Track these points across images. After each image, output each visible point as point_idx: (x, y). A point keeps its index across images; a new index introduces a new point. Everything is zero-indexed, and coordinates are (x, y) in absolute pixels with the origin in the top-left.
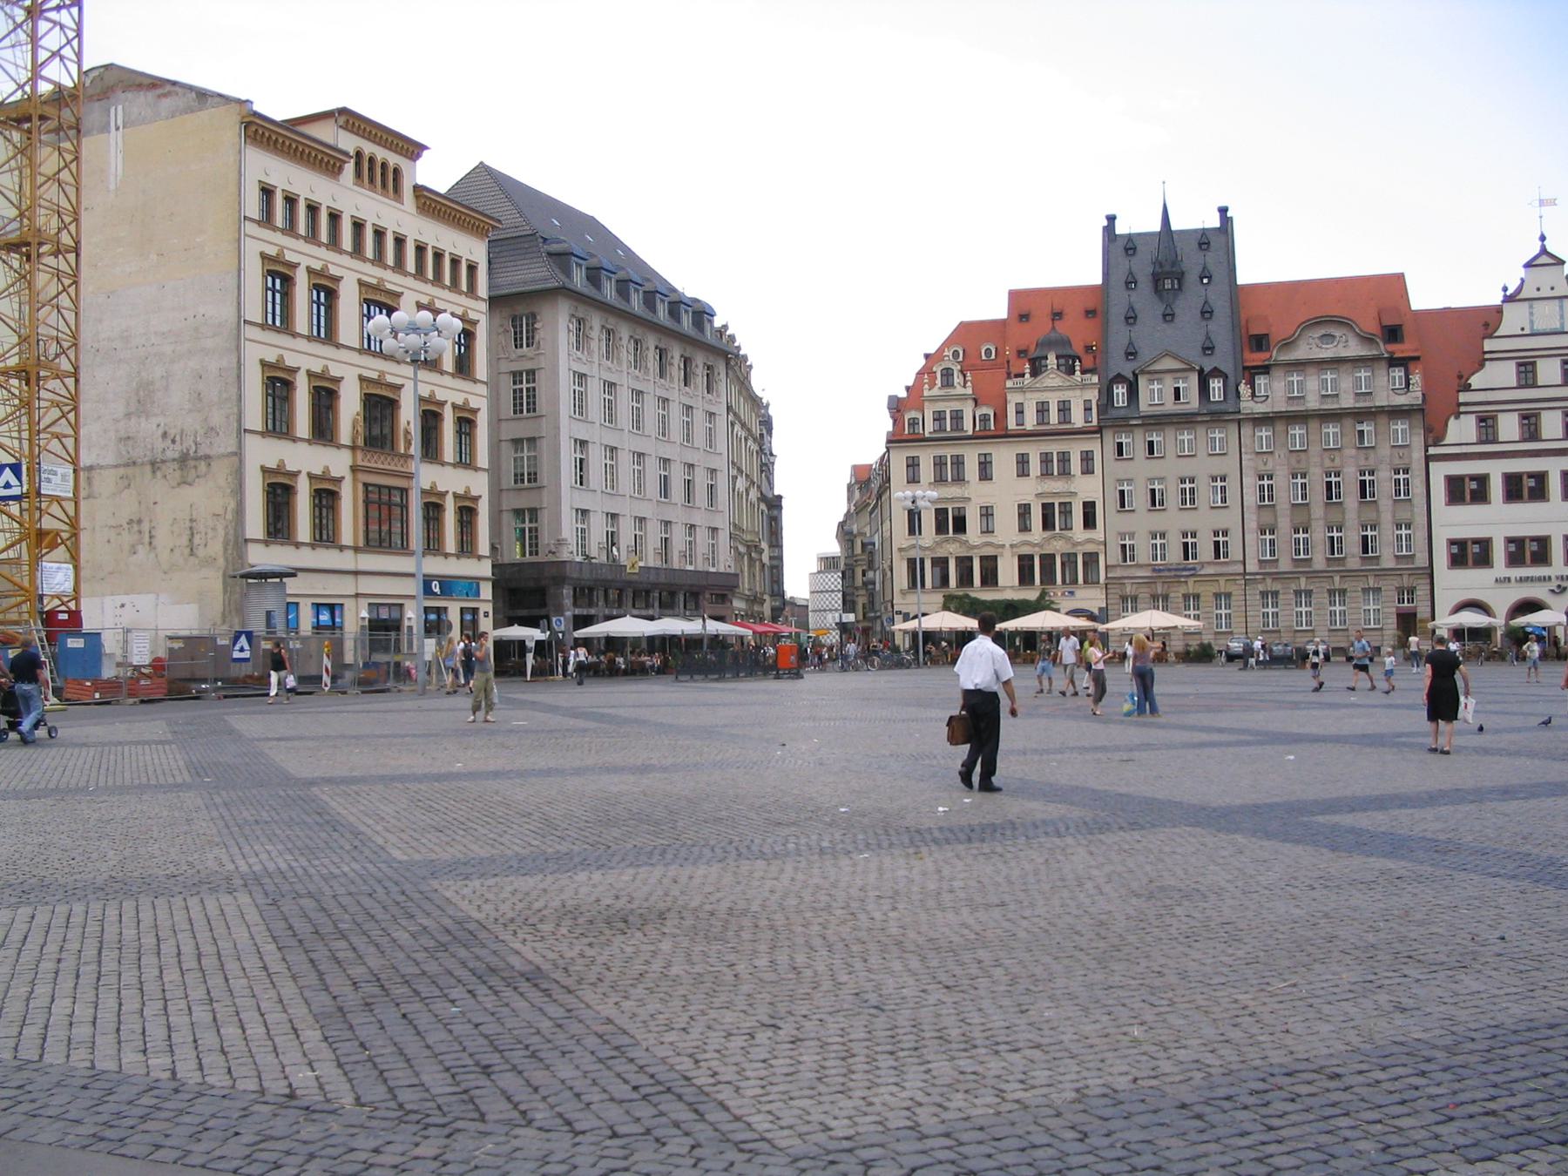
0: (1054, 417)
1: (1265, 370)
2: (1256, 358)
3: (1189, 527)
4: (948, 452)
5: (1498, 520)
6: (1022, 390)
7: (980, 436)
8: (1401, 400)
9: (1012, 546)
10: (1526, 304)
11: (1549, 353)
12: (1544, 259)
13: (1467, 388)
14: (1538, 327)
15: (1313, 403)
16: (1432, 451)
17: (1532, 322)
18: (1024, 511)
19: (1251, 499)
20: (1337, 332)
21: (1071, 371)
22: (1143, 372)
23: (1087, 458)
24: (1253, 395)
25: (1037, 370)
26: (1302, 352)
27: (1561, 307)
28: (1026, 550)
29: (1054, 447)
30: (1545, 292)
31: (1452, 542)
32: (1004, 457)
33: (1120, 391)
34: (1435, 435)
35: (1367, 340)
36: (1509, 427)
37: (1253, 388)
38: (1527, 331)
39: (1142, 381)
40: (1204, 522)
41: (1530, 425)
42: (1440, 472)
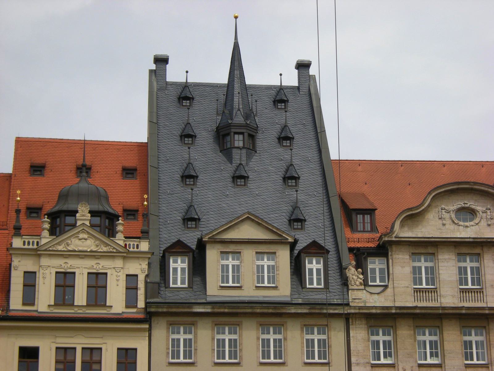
1: (382, 250)
2: (363, 239)
6: (36, 253)
15: (449, 298)
21: (111, 233)
22: (215, 241)
24: (365, 283)
26: (432, 227)
29: (79, 342)
37: (364, 273)
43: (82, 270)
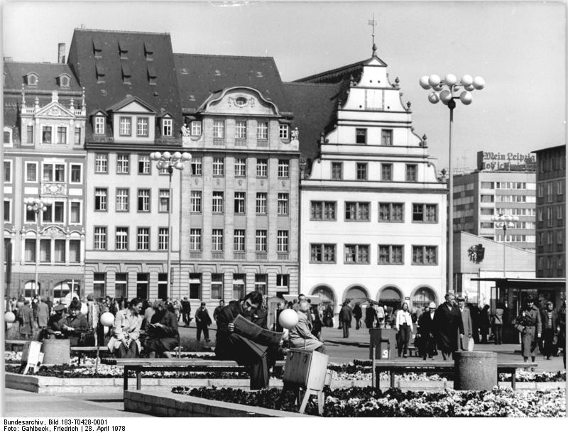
1: (200, 117)
3: (144, 224)
5: (339, 232)
11: (375, 123)
12: (375, 62)
13: (326, 143)
14: (370, 106)
16: (303, 183)
17: (366, 102)
19: (188, 206)
20: (248, 96)
25: (45, 101)
27: (383, 94)
28: (31, 235)
30: (375, 84)
31: (313, 246)
33: (100, 122)
34: (309, 169)
36: (349, 170)
38: (363, 109)
39: (116, 118)
40: (154, 220)
42: (308, 197)
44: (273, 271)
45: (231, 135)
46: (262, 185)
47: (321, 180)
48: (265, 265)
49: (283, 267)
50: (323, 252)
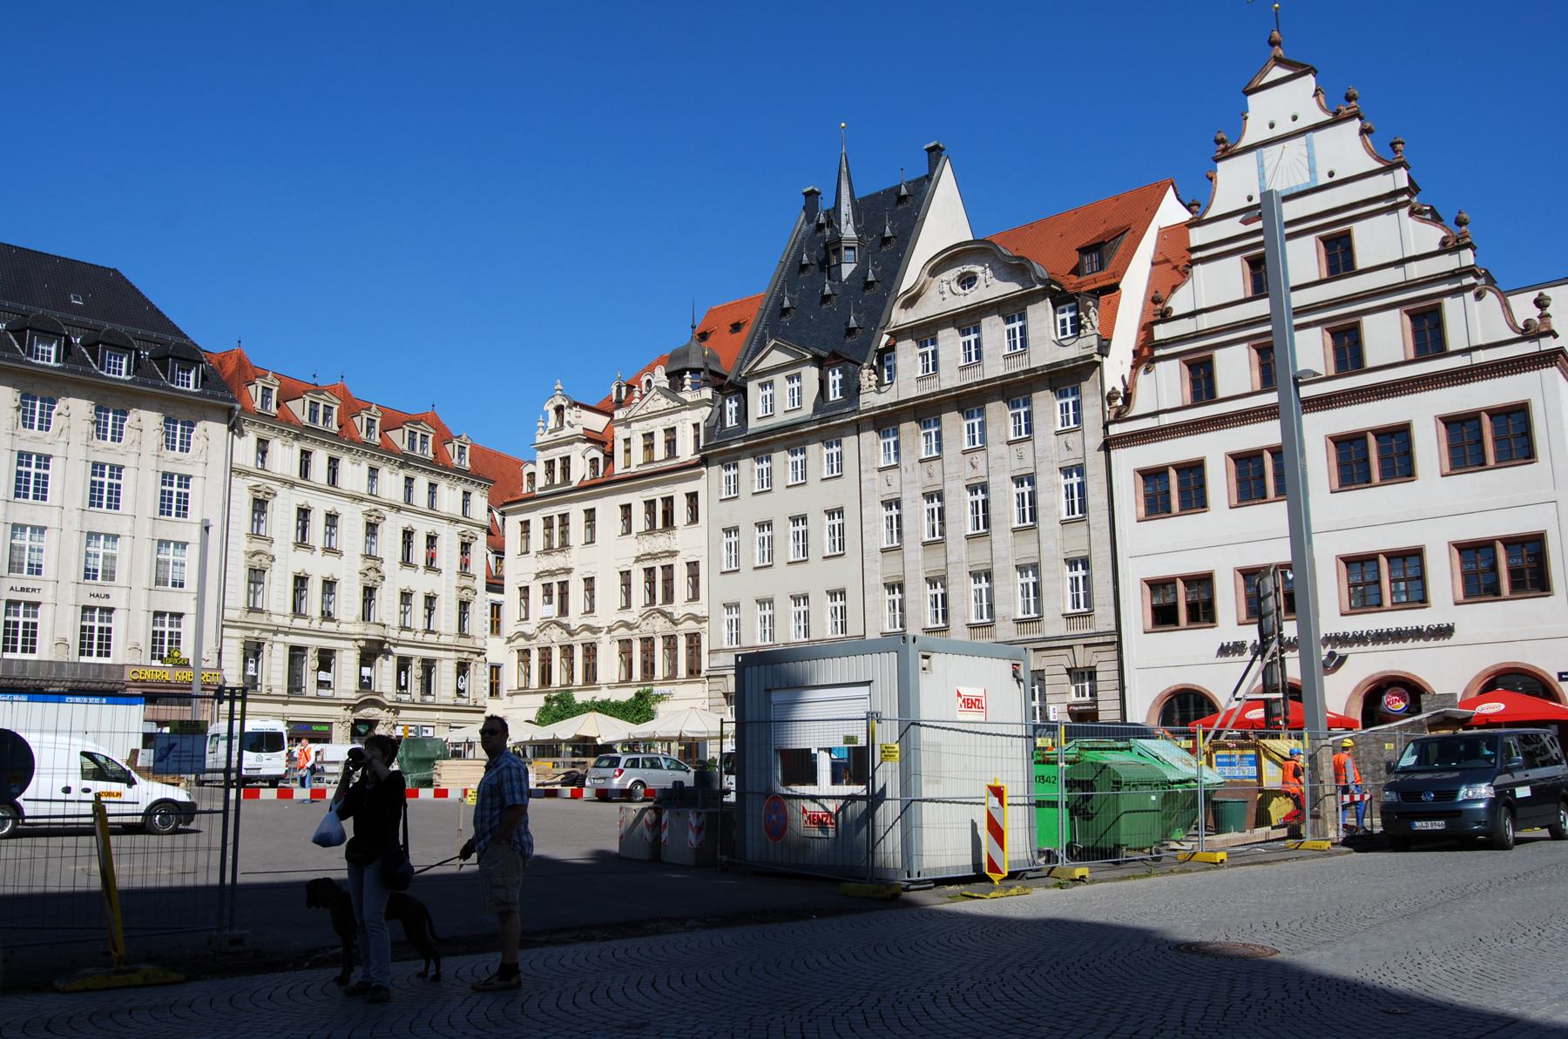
0: (660, 451)
4: (555, 511)
6: (626, 423)
7: (592, 487)
8: (1072, 351)
9: (610, 630)
10: (1252, 155)
13: (1165, 317)
18: (626, 575)
22: (753, 375)
23: (692, 497)
24: (880, 383)
27: (1309, 145)
32: (608, 508)
33: (731, 406)
35: (1016, 268)
36: (1235, 370)
41: (1270, 358)
42: (1129, 461)
43: (658, 427)
44: (1056, 660)
45: (953, 362)
46: (1021, 458)
47: (1155, 414)
48: (1035, 650)
49: (1079, 650)
50: (1181, 603)
